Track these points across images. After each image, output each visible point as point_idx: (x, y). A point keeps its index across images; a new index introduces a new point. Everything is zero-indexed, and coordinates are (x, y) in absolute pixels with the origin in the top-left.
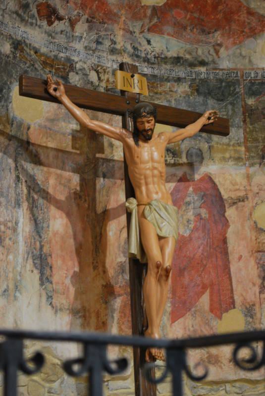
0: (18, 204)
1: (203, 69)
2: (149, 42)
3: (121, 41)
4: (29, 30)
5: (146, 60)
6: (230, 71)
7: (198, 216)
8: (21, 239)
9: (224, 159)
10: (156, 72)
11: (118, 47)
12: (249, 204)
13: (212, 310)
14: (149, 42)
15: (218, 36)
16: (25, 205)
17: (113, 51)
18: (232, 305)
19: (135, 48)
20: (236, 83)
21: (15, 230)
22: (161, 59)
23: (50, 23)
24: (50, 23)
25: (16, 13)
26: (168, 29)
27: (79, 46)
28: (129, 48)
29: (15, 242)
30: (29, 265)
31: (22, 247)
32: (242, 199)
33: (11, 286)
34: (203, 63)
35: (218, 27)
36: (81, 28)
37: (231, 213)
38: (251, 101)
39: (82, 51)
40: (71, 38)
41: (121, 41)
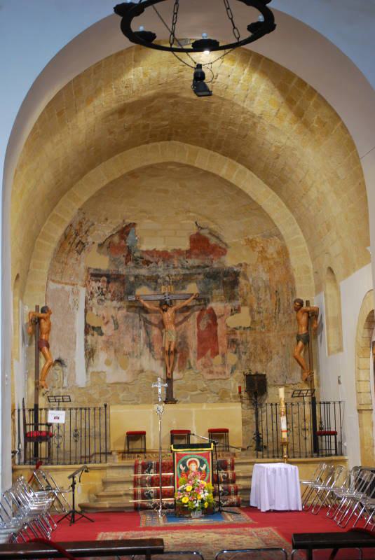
0: (140, 328)
1: (208, 269)
2: (187, 262)
3: (176, 263)
5: (187, 268)
6: (217, 268)
7: (208, 323)
8: (142, 339)
9: (217, 301)
10: (191, 272)
11: (176, 266)
12: (225, 317)
14: (187, 262)
15: (212, 256)
16: (143, 328)
17: (174, 268)
18: (217, 353)
19: (182, 265)
20: (218, 273)
21: (140, 337)
22: (193, 267)
23: (148, 265)
24: (148, 265)
25: (135, 267)
26: (193, 256)
27: (160, 269)
28: (180, 265)
29: (140, 340)
31: (142, 341)
32: (222, 316)
33: (139, 354)
34: (208, 266)
35: (211, 253)
36: (160, 263)
37: (219, 321)
38: (225, 279)
39: (162, 272)
41: (176, 263)
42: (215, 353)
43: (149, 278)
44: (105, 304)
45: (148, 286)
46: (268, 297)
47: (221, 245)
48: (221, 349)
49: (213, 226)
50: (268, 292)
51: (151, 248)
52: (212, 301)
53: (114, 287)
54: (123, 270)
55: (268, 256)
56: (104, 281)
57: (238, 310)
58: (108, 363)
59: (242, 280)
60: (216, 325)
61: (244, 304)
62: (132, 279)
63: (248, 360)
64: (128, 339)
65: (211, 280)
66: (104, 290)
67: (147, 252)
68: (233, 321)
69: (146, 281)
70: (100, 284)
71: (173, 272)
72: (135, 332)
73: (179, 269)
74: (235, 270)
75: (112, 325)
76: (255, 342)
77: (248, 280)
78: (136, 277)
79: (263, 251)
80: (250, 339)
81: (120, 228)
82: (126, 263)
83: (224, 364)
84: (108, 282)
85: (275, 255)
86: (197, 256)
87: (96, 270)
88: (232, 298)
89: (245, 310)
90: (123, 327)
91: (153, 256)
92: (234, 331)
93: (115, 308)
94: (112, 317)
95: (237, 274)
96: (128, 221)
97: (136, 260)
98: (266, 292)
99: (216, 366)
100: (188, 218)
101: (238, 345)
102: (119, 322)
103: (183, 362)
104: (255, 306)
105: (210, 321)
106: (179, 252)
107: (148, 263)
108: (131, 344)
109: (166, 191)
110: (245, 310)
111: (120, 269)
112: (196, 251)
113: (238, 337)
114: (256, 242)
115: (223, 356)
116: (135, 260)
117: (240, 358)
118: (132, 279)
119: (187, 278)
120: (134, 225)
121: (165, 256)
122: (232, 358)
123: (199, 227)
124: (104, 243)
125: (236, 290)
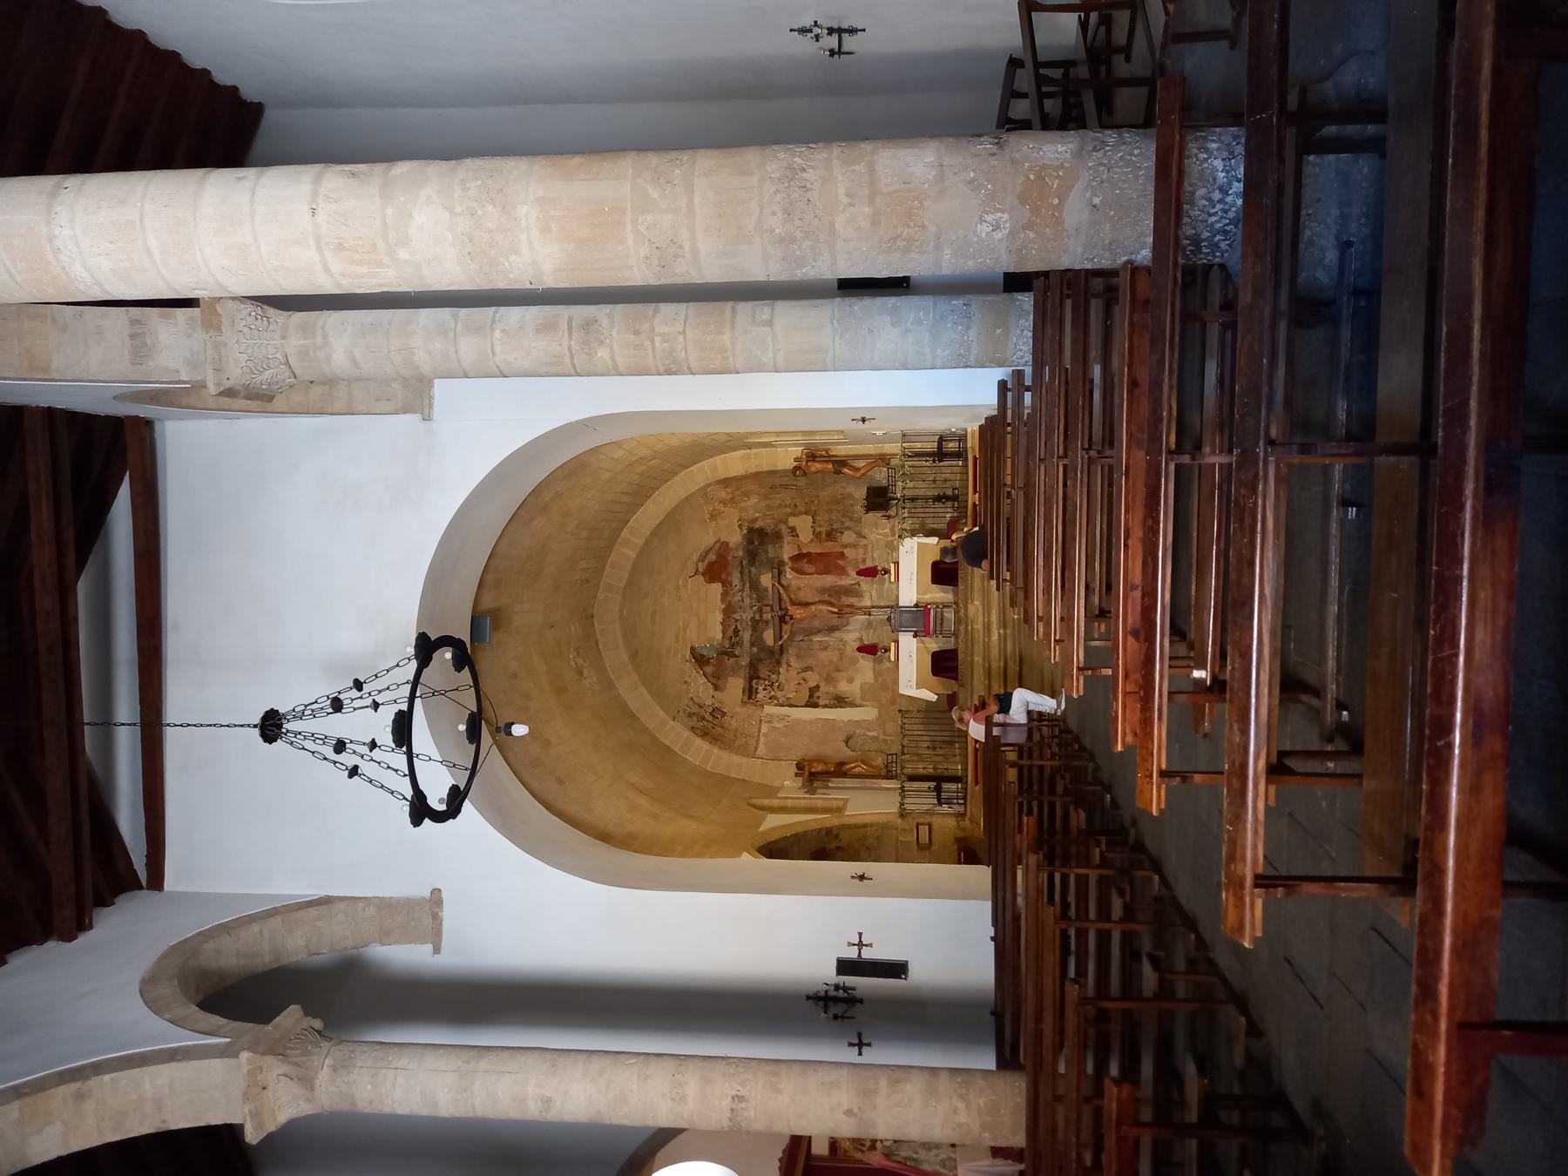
0: (811, 640)
1: (744, 562)
4: (745, 640)
5: (743, 586)
7: (806, 563)
9: (782, 552)
13: (844, 560)
16: (811, 637)
17: (743, 601)
18: (843, 552)
20: (749, 550)
21: (821, 641)
22: (742, 579)
26: (730, 579)
27: (744, 617)
30: (833, 635)
31: (826, 638)
32: (799, 546)
34: (741, 562)
35: (727, 560)
36: (737, 616)
40: (742, 620)
42: (842, 555)
43: (754, 629)
44: (784, 682)
45: (763, 630)
46: (778, 496)
47: (717, 548)
48: (836, 550)
49: (695, 558)
50: (771, 496)
51: (720, 627)
52: (782, 557)
53: (763, 672)
54: (745, 661)
55: (730, 497)
56: (757, 683)
57: (793, 529)
58: (851, 680)
59: (757, 526)
60: (809, 554)
61: (785, 522)
62: (755, 649)
63: (851, 519)
64: (824, 656)
65: (757, 558)
66: (767, 683)
67: (724, 632)
68: (805, 535)
69: (757, 634)
70: (761, 688)
71: (747, 601)
72: (816, 646)
73: (744, 594)
74: (745, 532)
75: (808, 674)
76: (830, 512)
77: (758, 517)
78: (752, 645)
79: (724, 502)
80: (827, 517)
81: (696, 665)
82: (737, 657)
83: (854, 546)
84: (759, 678)
85: (729, 490)
86: (729, 574)
87: (744, 692)
88: (778, 536)
89: (792, 521)
90: (810, 662)
91: (729, 625)
92: (817, 535)
93: (787, 671)
94: (798, 673)
95: (750, 530)
96: (688, 655)
97: (734, 645)
98: (771, 499)
99: (857, 555)
100: (685, 586)
101: (832, 529)
102: (805, 665)
103: (852, 592)
104: (789, 510)
105: (805, 561)
106: (725, 595)
107: (736, 632)
108: (829, 652)
109: (654, 614)
110: (792, 521)
111: (744, 664)
112: (723, 576)
113: (823, 529)
114: (714, 510)
115: (845, 546)
116: (733, 646)
117: (848, 528)
118: (755, 649)
119: (755, 586)
120: (692, 648)
121: (728, 611)
122: (848, 537)
123: (695, 574)
124: (712, 684)
125: (769, 531)
